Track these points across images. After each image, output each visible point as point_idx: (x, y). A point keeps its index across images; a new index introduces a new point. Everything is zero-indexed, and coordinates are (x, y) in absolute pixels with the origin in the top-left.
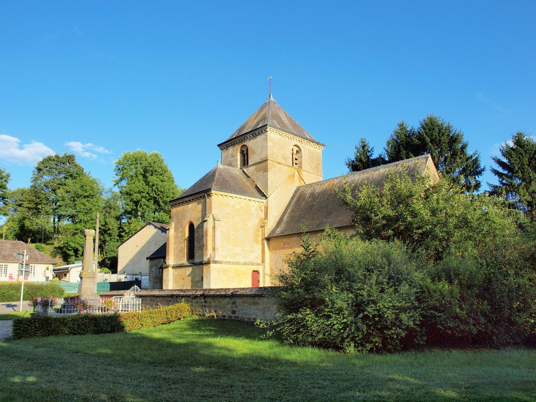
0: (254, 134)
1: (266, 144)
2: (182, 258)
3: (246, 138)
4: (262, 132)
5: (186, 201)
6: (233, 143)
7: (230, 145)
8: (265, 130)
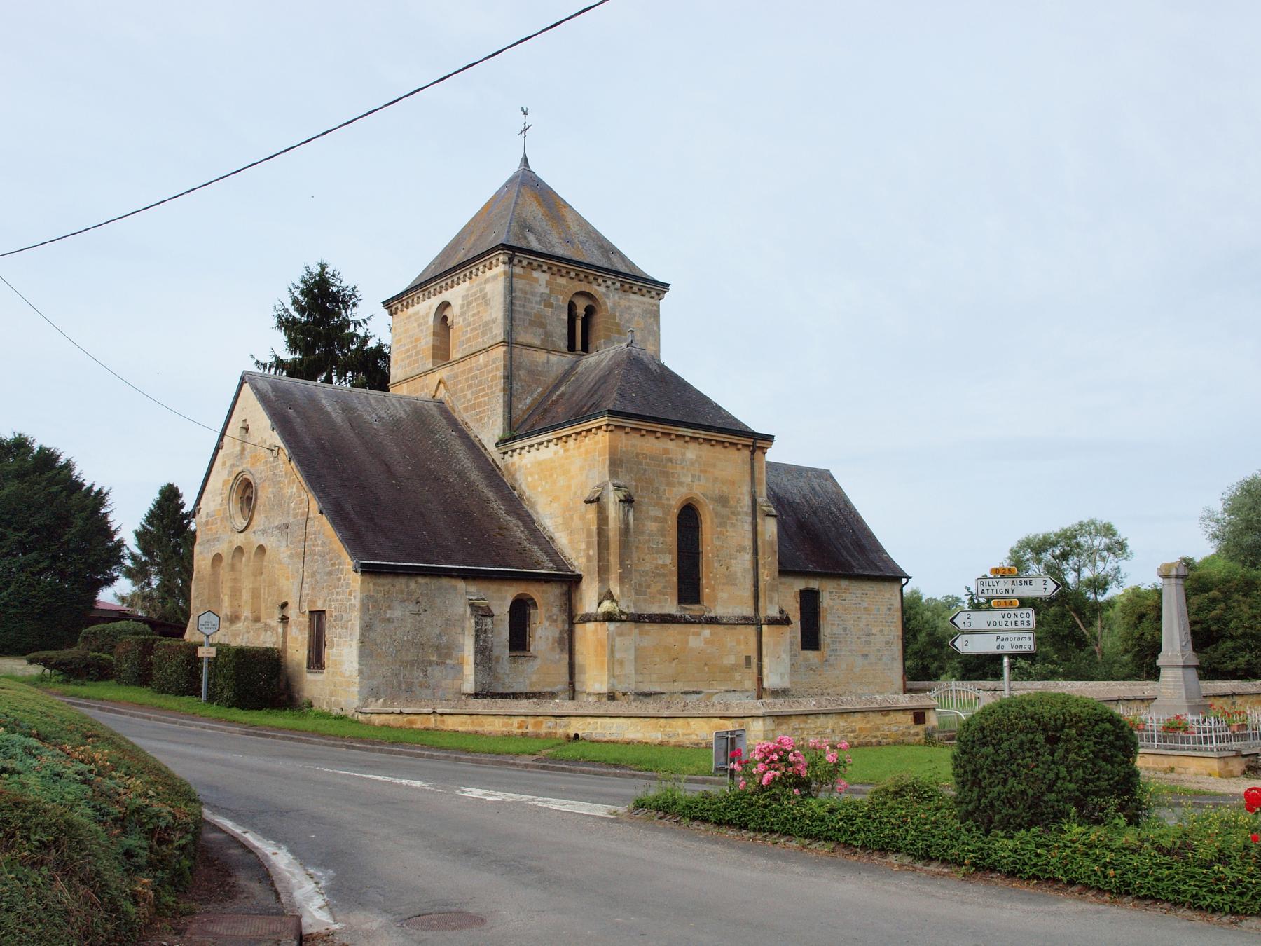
0: (627, 286)
1: (655, 328)
2: (662, 597)
3: (600, 281)
4: (649, 292)
5: (677, 436)
6: (555, 269)
7: (545, 268)
8: (658, 294)
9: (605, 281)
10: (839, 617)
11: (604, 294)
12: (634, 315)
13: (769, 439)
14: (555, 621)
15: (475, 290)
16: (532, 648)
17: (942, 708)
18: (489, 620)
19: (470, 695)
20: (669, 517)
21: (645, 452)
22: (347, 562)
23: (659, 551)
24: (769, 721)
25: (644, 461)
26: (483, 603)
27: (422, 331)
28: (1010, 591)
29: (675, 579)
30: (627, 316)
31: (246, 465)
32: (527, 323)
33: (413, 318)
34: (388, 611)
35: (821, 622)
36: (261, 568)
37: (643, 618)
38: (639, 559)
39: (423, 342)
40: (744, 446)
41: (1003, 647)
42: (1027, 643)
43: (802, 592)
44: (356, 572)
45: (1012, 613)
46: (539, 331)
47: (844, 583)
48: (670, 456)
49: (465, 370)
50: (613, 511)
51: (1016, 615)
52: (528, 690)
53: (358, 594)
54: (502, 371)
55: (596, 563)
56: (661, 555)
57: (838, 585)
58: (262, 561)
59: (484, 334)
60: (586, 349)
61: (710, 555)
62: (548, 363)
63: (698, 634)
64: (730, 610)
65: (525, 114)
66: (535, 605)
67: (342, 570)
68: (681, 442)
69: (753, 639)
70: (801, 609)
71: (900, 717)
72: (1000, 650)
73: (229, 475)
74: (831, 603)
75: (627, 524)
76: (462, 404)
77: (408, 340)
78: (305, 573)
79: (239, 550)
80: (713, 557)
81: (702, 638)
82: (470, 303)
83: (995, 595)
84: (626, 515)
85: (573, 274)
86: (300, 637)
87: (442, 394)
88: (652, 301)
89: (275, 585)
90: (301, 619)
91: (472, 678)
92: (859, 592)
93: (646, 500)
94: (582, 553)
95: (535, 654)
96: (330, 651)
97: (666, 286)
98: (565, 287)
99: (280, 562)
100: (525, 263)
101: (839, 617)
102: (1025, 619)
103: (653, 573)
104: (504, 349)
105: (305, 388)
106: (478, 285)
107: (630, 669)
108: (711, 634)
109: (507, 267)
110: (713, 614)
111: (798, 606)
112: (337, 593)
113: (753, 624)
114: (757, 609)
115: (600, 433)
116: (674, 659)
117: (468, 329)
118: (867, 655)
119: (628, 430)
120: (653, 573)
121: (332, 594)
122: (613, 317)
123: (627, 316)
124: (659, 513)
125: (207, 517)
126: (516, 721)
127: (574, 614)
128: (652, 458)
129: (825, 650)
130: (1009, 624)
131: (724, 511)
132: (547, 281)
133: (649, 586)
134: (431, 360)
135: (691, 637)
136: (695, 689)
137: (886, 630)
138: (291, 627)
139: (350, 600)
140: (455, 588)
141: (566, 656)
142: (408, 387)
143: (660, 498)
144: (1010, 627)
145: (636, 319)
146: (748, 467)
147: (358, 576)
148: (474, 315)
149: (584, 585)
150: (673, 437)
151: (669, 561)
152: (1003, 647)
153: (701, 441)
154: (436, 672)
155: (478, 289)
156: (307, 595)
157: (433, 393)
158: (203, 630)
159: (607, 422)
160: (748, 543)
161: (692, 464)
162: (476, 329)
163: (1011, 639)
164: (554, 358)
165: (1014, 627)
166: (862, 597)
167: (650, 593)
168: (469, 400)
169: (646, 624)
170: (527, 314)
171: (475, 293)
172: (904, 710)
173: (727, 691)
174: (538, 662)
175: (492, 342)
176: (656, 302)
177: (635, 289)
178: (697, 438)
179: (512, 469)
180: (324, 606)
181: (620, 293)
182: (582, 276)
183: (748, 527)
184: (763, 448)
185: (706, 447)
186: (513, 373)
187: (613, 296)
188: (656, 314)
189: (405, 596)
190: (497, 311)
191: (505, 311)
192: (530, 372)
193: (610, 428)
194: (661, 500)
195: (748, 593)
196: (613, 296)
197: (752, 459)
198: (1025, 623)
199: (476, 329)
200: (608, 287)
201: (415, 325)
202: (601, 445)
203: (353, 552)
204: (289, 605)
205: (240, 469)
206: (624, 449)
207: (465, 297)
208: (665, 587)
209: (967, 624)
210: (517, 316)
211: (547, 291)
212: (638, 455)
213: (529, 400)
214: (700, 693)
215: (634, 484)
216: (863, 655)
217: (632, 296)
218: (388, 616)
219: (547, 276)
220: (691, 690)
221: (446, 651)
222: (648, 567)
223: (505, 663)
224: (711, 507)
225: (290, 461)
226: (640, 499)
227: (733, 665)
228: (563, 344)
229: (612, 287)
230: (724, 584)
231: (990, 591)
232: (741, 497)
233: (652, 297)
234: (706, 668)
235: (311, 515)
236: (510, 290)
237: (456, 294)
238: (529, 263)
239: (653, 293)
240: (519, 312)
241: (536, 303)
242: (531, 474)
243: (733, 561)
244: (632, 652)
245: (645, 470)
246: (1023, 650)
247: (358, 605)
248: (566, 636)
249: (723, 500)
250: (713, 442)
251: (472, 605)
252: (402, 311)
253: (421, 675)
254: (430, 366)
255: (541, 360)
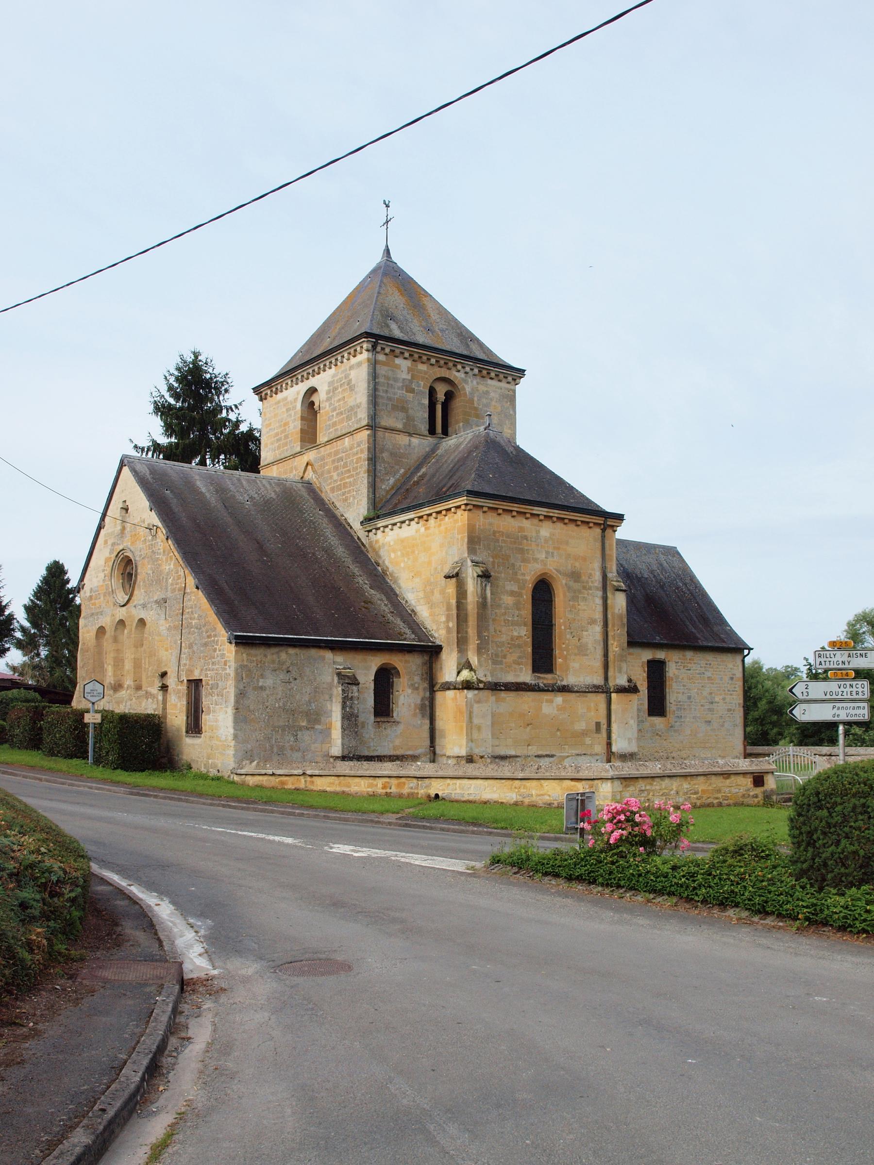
1: (511, 412)
2: (517, 667)
3: (459, 367)
4: (506, 378)
5: (532, 515)
6: (416, 356)
7: (407, 355)
8: (514, 380)
9: (463, 367)
10: (684, 686)
11: (463, 379)
12: (491, 400)
13: (620, 518)
14: (417, 689)
15: (340, 376)
16: (395, 714)
17: (780, 772)
18: (355, 688)
19: (338, 757)
20: (524, 592)
21: (501, 530)
22: (222, 634)
23: (514, 624)
24: (617, 783)
25: (501, 538)
26: (349, 672)
27: (290, 415)
28: (846, 663)
29: (530, 650)
30: (484, 401)
31: (126, 543)
32: (390, 407)
33: (282, 404)
34: (261, 680)
35: (667, 690)
36: (142, 640)
37: (500, 686)
38: (495, 631)
39: (292, 425)
40: (595, 524)
41: (838, 716)
42: (861, 712)
43: (649, 662)
44: (231, 643)
45: (848, 683)
46: (402, 415)
47: (689, 654)
48: (526, 534)
49: (331, 453)
50: (472, 586)
51: (851, 686)
52: (392, 753)
53: (232, 664)
54: (366, 453)
55: (455, 634)
56: (516, 627)
57: (683, 656)
58: (143, 633)
59: (349, 418)
60: (445, 432)
61: (563, 627)
62: (410, 445)
63: (551, 701)
64: (581, 679)
65: (388, 206)
66: (398, 674)
67: (217, 641)
68: (535, 521)
69: (603, 706)
70: (648, 678)
71: (740, 780)
72: (836, 718)
73: (111, 552)
74: (676, 672)
75: (484, 597)
76: (328, 485)
77: (277, 425)
78: (183, 645)
79: (121, 622)
80: (565, 629)
81: (554, 704)
82: (336, 389)
83: (832, 666)
84: (484, 590)
85: (433, 361)
86: (179, 704)
87: (310, 475)
88: (508, 386)
89: (155, 655)
90: (179, 687)
91: (339, 742)
92: (703, 663)
93: (503, 575)
94: (442, 626)
95: (398, 720)
96: (207, 717)
97: (521, 372)
98: (426, 373)
99: (159, 635)
100: (387, 350)
101: (684, 686)
102: (860, 690)
103: (509, 644)
104: (368, 432)
105: (182, 470)
106: (343, 372)
107: (486, 734)
108: (563, 701)
109: (371, 354)
110: (565, 683)
111: (645, 675)
112: (213, 663)
113: (603, 692)
114: (606, 679)
115: (459, 512)
116: (528, 725)
117: (334, 414)
118: (710, 722)
119: (485, 509)
120: (509, 644)
121: (208, 664)
122: (471, 401)
123: (484, 401)
124: (515, 588)
125: (91, 592)
126: (380, 782)
127: (434, 682)
128: (508, 537)
129: (671, 717)
130: (845, 694)
131: (577, 586)
132: (408, 367)
133: (505, 657)
134: (299, 443)
135: (544, 704)
136: (548, 753)
137: (728, 698)
138: (170, 694)
139: (225, 669)
140: (323, 658)
141: (428, 722)
142: (278, 469)
143: (516, 574)
144: (845, 697)
145: (493, 403)
146: (598, 545)
147: (233, 647)
148: (339, 400)
149: (444, 655)
150: (528, 515)
151: (524, 633)
152: (838, 716)
153: (555, 519)
154: (306, 737)
155: (343, 375)
156: (185, 664)
157: (301, 475)
158: (89, 698)
159: (465, 502)
160: (598, 615)
161: (546, 541)
162: (341, 413)
163: (847, 708)
164: (415, 441)
165: (849, 696)
166: (705, 667)
167: (506, 663)
168: (336, 481)
169: (502, 692)
170: (389, 399)
171: (341, 379)
172: (745, 774)
173: (578, 755)
174: (400, 728)
175: (356, 426)
176: (512, 387)
177: (493, 375)
178: (551, 517)
179: (377, 546)
180: (200, 675)
181: (478, 379)
182: (442, 362)
183: (599, 601)
184: (613, 526)
185: (559, 525)
186: (378, 455)
187: (472, 382)
188: (512, 399)
189: (276, 666)
190: (361, 397)
191: (368, 396)
192: (392, 454)
193: (469, 507)
194: (517, 575)
195: (598, 664)
196: (472, 382)
197: (603, 537)
198: (860, 694)
199: (341, 413)
200: (466, 373)
201: (284, 410)
202: (460, 524)
203: (228, 625)
204: (169, 674)
205: (121, 547)
206: (482, 527)
207: (330, 383)
208: (520, 657)
209: (805, 694)
210: (380, 401)
211: (409, 377)
212: (494, 532)
213: (392, 481)
214: (552, 756)
215: (491, 560)
216: (706, 722)
217: (490, 382)
218: (260, 684)
219: (408, 363)
220: (544, 753)
221: (315, 717)
222: (504, 638)
223: (370, 727)
224: (564, 582)
225: (167, 539)
226: (497, 574)
227: (584, 730)
228: (424, 427)
229: (471, 373)
230: (575, 655)
231: (827, 663)
232: (593, 572)
233: (508, 383)
234: (558, 733)
235: (188, 590)
236: (374, 376)
237: (322, 380)
238: (391, 350)
239: (510, 379)
240: (382, 397)
241: (398, 389)
242: (394, 551)
243: (585, 633)
244: (490, 717)
245: (502, 547)
246: (858, 718)
247: (232, 674)
248: (427, 703)
249: (575, 576)
250: (566, 521)
251: (339, 674)
252: (271, 396)
253: (292, 739)
254: (298, 449)
255: (403, 443)
